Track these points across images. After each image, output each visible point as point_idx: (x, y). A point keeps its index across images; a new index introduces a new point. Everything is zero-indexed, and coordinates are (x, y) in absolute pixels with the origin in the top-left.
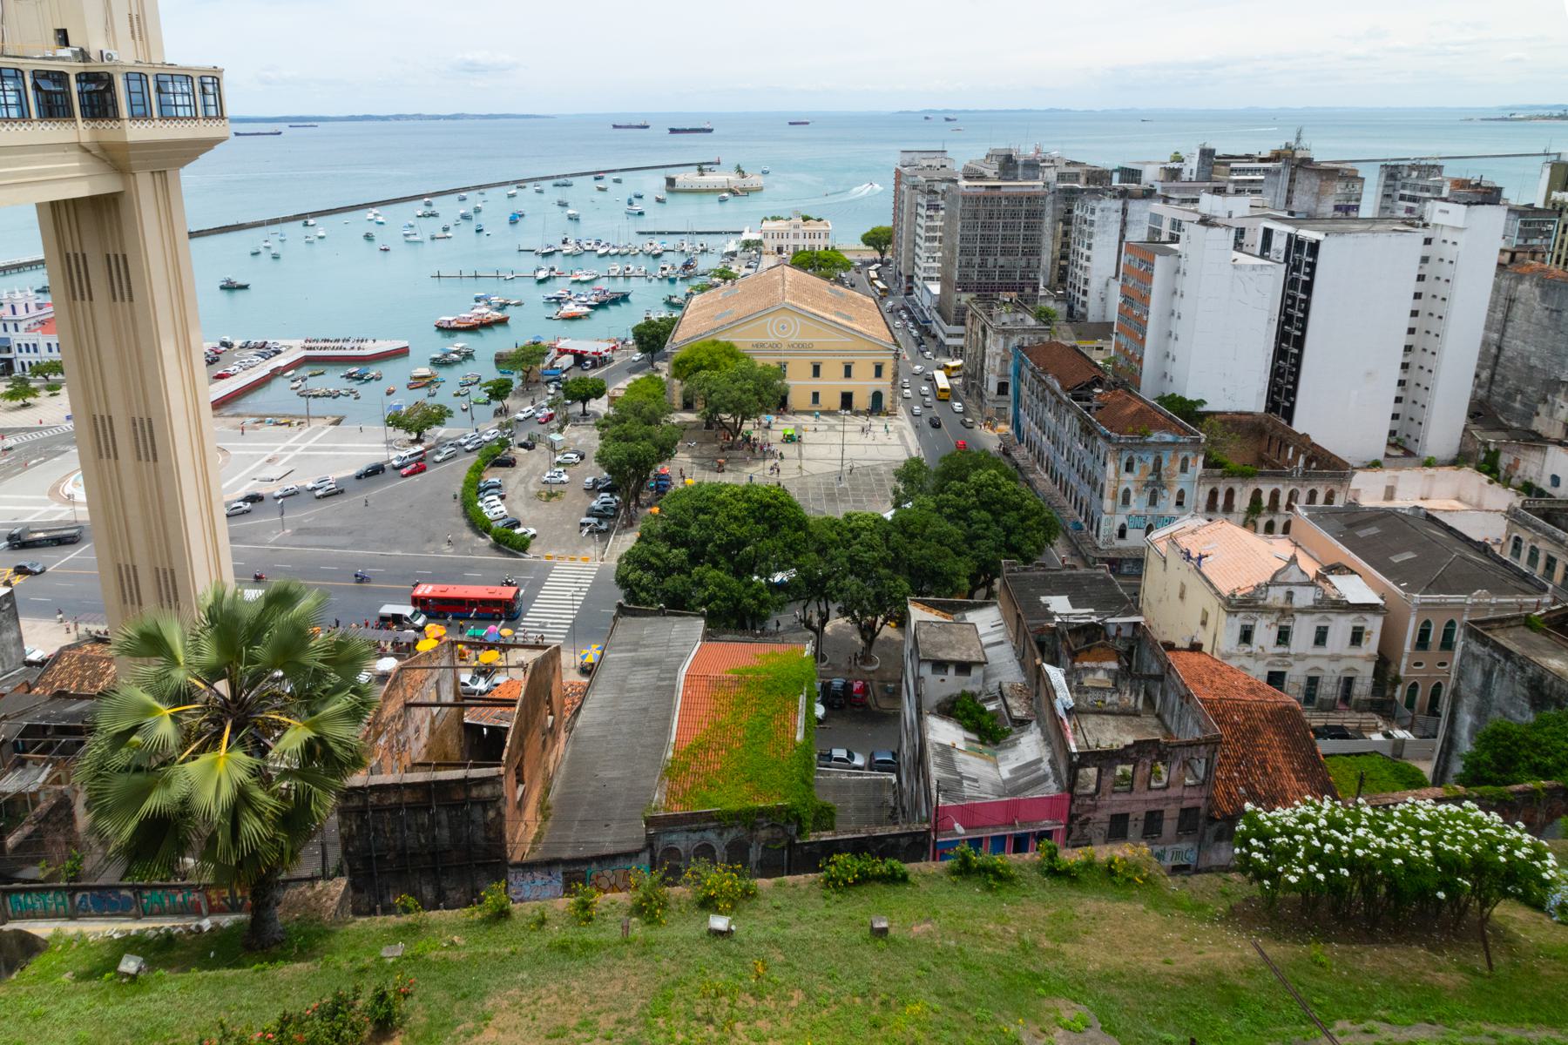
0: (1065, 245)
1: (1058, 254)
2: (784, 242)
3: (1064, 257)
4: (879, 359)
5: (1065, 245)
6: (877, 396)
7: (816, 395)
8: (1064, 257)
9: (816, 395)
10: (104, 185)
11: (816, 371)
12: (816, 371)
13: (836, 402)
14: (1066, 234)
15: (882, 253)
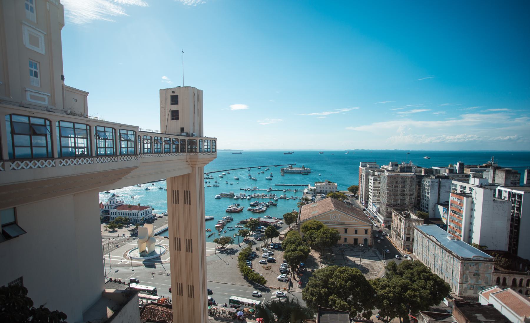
0: (419, 193)
1: (417, 196)
2: (323, 189)
3: (419, 196)
4: (366, 228)
5: (419, 193)
6: (366, 240)
7: (346, 239)
8: (419, 196)
9: (346, 239)
10: (187, 171)
11: (346, 231)
12: (346, 231)
13: (352, 242)
14: (419, 189)
15: (355, 194)
